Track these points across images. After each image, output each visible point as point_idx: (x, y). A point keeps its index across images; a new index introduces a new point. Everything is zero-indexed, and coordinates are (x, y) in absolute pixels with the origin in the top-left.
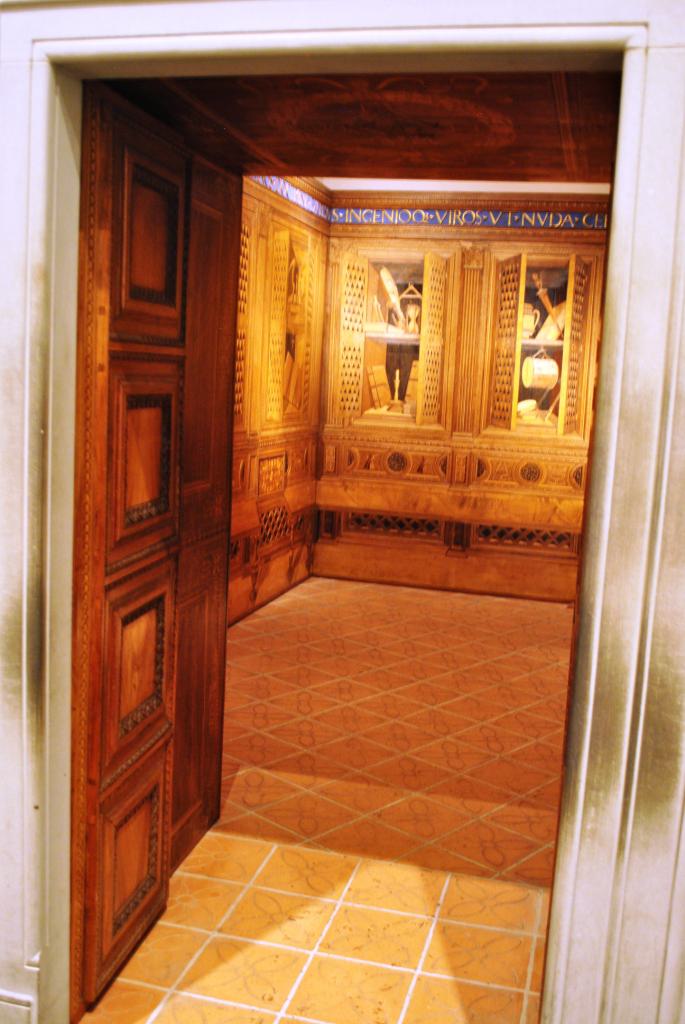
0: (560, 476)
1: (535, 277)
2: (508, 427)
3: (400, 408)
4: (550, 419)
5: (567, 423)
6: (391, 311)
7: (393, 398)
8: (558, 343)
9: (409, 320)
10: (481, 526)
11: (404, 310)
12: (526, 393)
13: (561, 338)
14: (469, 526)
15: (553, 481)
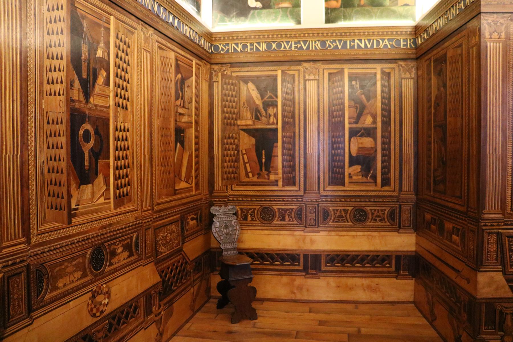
0: (380, 217)
1: (354, 83)
2: (343, 184)
3: (266, 177)
4: (371, 177)
5: (383, 180)
6: (257, 110)
7: (261, 170)
8: (373, 126)
9: (270, 116)
10: (328, 255)
11: (266, 110)
12: (353, 161)
13: (374, 122)
14: (320, 255)
15: (376, 220)
